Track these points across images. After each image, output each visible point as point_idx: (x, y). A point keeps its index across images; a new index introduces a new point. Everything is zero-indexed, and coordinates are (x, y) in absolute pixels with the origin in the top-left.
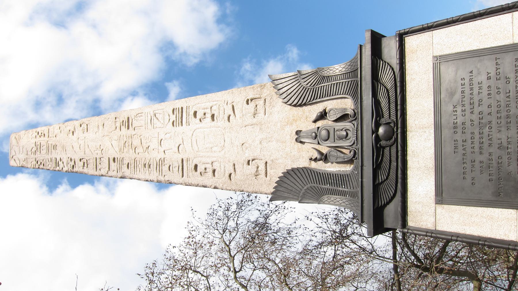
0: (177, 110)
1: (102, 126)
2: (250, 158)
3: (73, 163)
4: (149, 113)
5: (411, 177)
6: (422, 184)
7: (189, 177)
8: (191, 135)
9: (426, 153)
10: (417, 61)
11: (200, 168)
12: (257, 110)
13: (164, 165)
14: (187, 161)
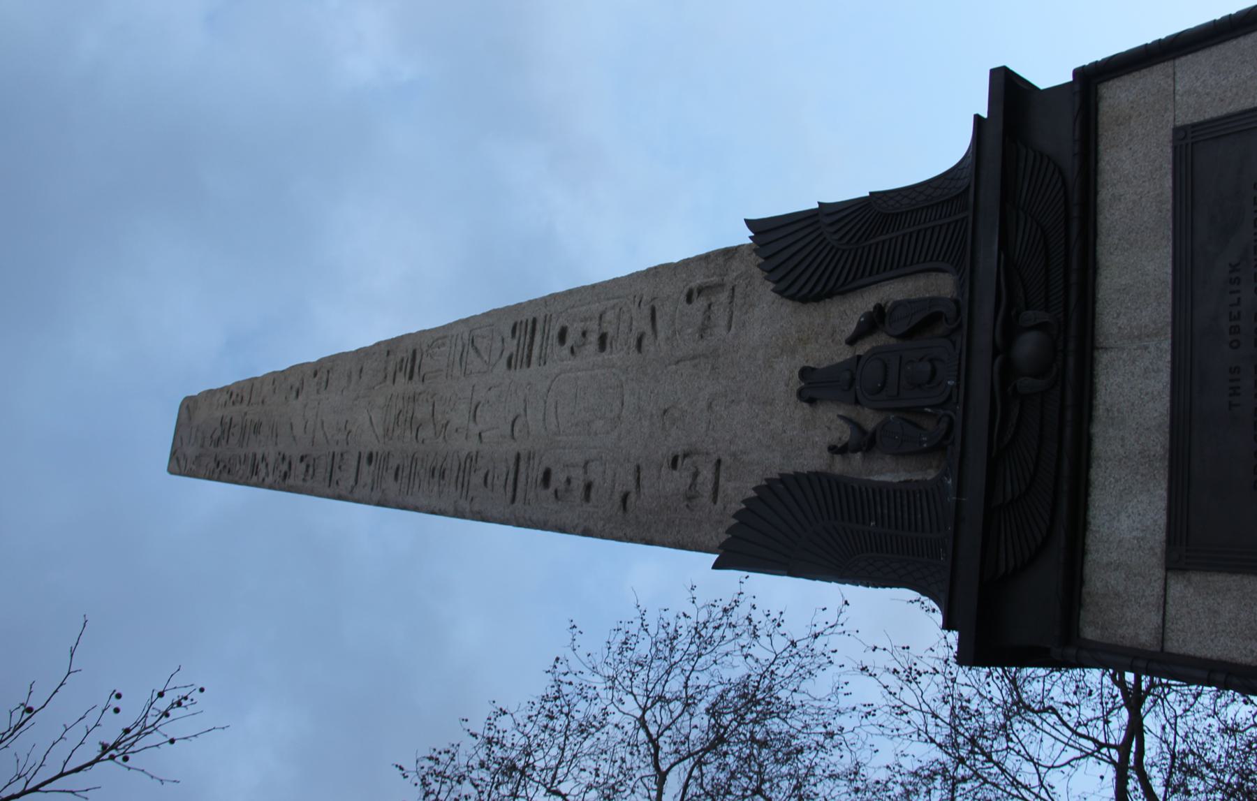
1: (358, 373)
2: (679, 449)
3: (284, 467)
4: (460, 336)
5: (1100, 487)
6: (1129, 507)
7: (527, 501)
8: (545, 390)
9: (1148, 411)
10: (1129, 147)
11: (558, 479)
12: (709, 317)
13: (475, 471)
14: (529, 459)
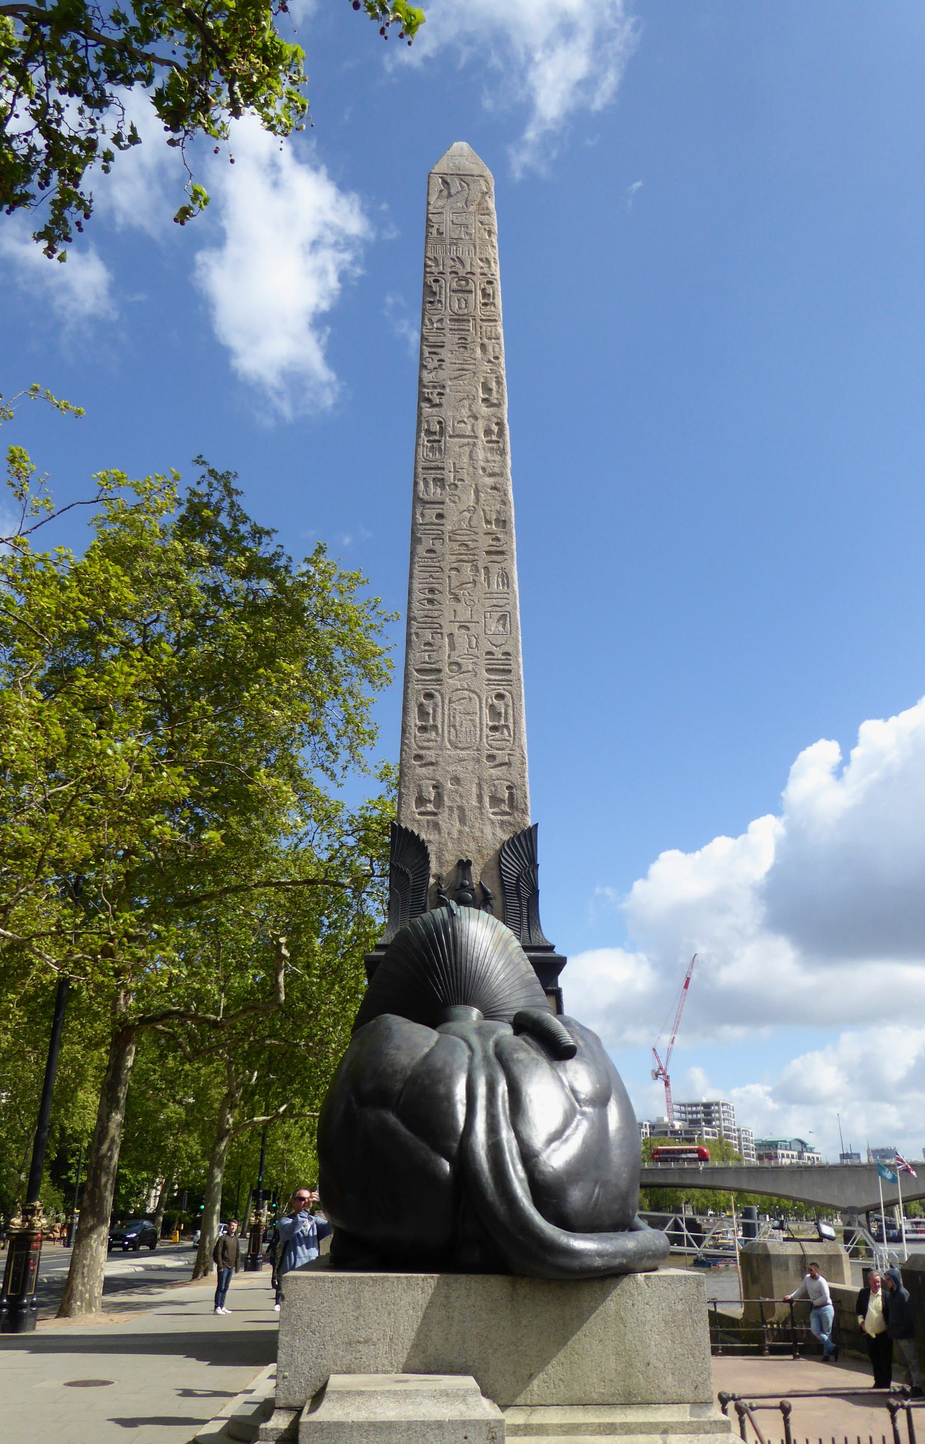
0: (506, 662)
14: (438, 680)
